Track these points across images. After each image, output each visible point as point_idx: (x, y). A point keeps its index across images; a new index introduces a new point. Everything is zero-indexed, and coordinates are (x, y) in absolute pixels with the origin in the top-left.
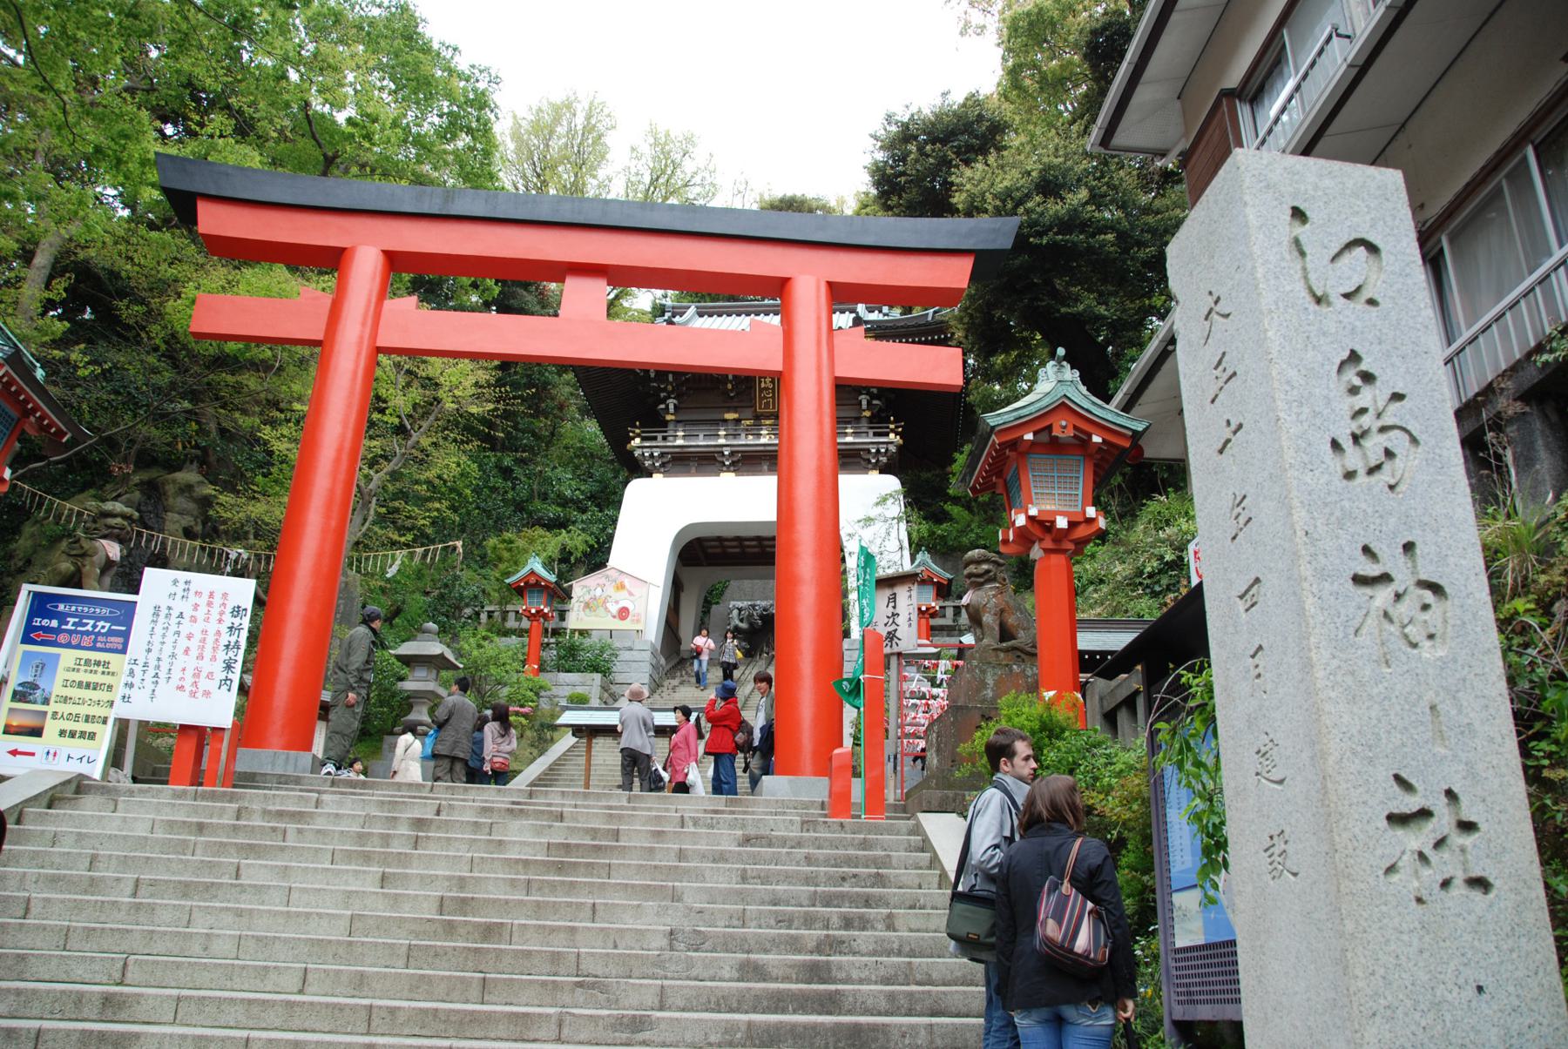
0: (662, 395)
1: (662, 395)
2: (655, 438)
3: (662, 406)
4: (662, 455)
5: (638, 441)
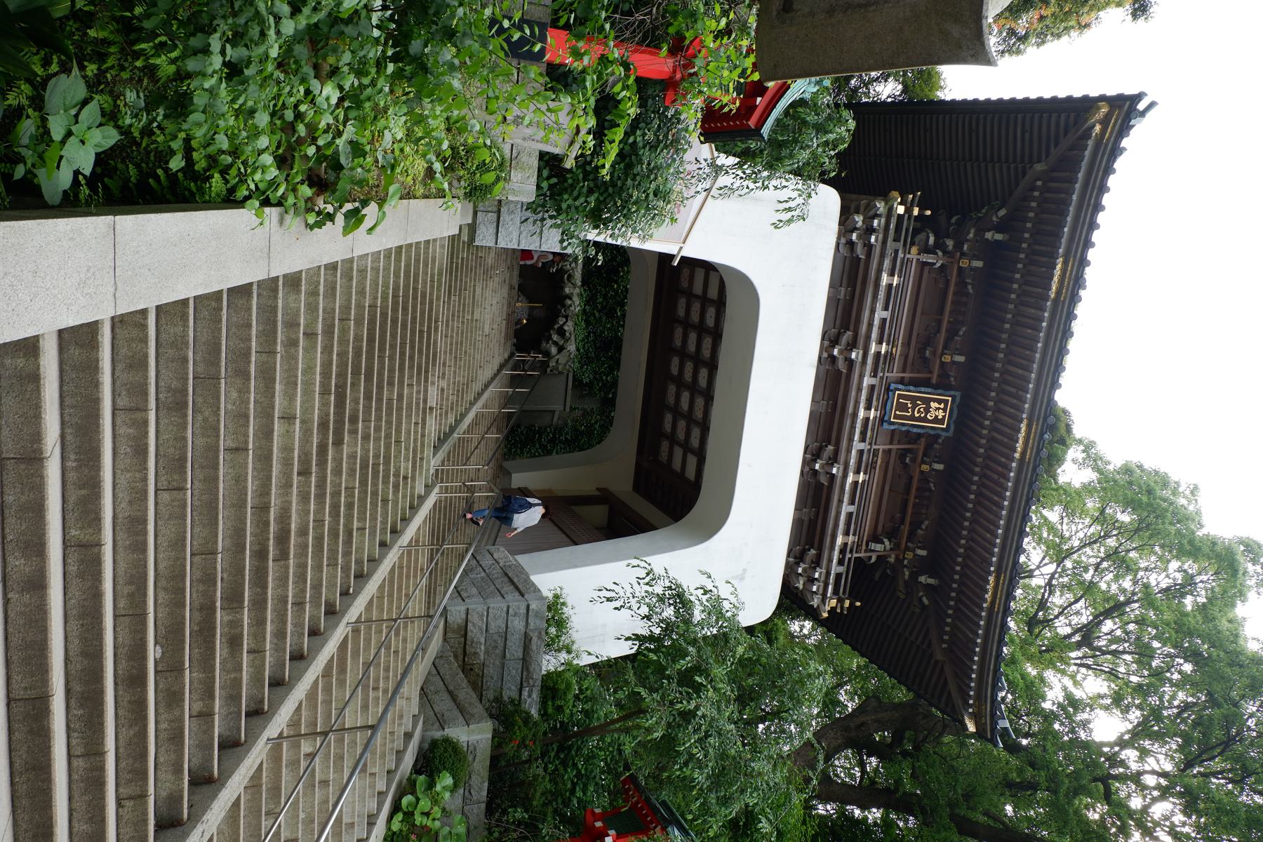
0: (950, 243)
1: (950, 243)
2: (896, 239)
3: (932, 240)
4: (869, 247)
5: (901, 210)
